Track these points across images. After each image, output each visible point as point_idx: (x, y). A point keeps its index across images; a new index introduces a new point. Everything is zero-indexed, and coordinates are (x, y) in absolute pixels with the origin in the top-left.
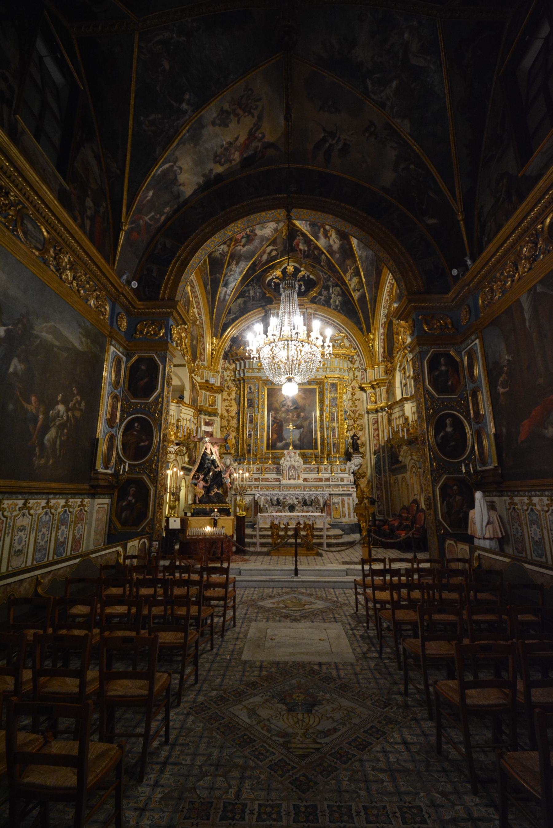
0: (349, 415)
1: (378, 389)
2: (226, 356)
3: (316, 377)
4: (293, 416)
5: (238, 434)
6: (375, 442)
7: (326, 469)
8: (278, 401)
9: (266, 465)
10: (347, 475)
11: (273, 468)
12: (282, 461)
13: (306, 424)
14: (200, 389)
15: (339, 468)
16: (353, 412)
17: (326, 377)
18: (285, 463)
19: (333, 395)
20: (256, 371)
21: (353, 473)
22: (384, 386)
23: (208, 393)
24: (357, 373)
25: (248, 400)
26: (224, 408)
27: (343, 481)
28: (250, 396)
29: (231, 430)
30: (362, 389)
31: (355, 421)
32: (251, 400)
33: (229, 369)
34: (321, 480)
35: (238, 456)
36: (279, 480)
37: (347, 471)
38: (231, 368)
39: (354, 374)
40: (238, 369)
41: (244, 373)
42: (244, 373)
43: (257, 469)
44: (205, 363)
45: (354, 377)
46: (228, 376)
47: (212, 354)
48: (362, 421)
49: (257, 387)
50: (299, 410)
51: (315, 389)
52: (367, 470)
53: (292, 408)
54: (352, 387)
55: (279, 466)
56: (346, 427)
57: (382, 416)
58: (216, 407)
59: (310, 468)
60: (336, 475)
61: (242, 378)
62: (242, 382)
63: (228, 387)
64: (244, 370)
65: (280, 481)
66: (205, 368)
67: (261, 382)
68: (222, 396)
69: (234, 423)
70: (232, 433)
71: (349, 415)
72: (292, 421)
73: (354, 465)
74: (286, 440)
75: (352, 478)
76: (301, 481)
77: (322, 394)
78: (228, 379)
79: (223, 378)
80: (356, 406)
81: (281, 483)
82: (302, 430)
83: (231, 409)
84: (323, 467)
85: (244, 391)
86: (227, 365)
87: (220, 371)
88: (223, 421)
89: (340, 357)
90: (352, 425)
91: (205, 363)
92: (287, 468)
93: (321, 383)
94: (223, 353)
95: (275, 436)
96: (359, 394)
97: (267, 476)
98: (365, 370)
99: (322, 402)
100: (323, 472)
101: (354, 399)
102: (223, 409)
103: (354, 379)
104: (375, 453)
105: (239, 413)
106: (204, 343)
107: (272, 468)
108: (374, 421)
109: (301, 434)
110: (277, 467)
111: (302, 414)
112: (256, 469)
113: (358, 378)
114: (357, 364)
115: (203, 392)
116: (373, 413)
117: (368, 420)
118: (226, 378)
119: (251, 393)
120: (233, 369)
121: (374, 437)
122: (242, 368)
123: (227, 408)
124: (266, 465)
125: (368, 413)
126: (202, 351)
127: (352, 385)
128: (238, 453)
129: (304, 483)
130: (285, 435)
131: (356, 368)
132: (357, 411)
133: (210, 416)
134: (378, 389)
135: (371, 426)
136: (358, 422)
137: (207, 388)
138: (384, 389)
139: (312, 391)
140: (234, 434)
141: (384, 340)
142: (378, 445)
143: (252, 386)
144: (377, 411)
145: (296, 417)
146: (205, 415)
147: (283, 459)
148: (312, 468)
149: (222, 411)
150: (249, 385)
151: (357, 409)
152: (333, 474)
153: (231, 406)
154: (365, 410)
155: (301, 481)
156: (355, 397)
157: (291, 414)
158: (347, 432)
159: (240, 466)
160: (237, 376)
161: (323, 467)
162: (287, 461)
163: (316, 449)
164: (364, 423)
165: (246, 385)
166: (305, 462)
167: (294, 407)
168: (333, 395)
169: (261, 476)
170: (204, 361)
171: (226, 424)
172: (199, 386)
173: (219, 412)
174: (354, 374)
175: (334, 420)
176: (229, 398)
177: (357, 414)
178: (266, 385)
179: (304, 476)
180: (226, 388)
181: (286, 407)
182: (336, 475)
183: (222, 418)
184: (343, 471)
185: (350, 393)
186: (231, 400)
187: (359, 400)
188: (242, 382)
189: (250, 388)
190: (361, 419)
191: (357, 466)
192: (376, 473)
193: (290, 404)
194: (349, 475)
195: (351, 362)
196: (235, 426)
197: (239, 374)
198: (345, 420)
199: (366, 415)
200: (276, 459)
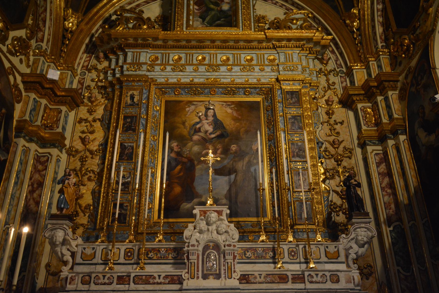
0: (326, 150)
1: (380, 98)
2: (92, 49)
3: (259, 80)
5: (100, 186)
6: (386, 198)
7: (293, 254)
8: (187, 124)
9: (149, 245)
10: (343, 267)
11: (167, 250)
12: (187, 233)
13: (241, 165)
14: (26, 90)
15: (322, 249)
16: (333, 144)
17: (278, 80)
18: (196, 235)
19: (293, 111)
20: (145, 67)
21: (355, 261)
22: (394, 89)
23: (44, 102)
24: (332, 79)
25: (125, 118)
26: (78, 134)
27: (338, 281)
28: (131, 111)
30: (347, 102)
31: (338, 162)
32: (132, 117)
33: (96, 69)
34: (283, 279)
35: (95, 229)
36: (179, 280)
37: (342, 258)
38: (100, 67)
39: (328, 80)
40: (113, 67)
41: (122, 72)
42: (122, 72)
43: (128, 254)
44: (44, 45)
45: (329, 85)
46: (93, 80)
47: (64, 37)
48: (353, 161)
49: (145, 96)
50: (226, 140)
51: (258, 103)
52: (374, 260)
53: (213, 136)
54: (327, 101)
55: (179, 245)
56: (323, 171)
57: (397, 148)
58: (60, 130)
59: (255, 250)
60: (320, 267)
61: (118, 79)
62: (117, 87)
63: (89, 98)
64: (122, 67)
65: (181, 283)
66: (43, 54)
67: (153, 88)
68: (76, 114)
69: (94, 164)
70: (89, 183)
71: (326, 150)
73: (356, 243)
74: (201, 197)
75: (356, 274)
76: (234, 283)
77: (271, 110)
78: (93, 85)
79: (82, 84)
80: (338, 133)
81: (185, 286)
82: (233, 176)
83: (91, 137)
84: (286, 248)
85: (120, 103)
86: (94, 61)
87: (79, 72)
88: (72, 159)
89: (302, 47)
90: (333, 169)
91: (44, 45)
92: (201, 248)
93: (269, 92)
94: (87, 41)
95: (178, 189)
96: (340, 112)
97: (150, 269)
98: (350, 73)
99: (272, 124)
100: (286, 259)
102: (76, 137)
103: (329, 88)
104: (389, 222)
105: (104, 145)
106: (46, 10)
107: (163, 251)
108: (377, 158)
109: (232, 185)
110: (175, 250)
111: (234, 147)
112: (126, 254)
114: (331, 65)
115: (33, 96)
116: (375, 144)
117: (365, 160)
118: (88, 82)
119: (133, 105)
120: (104, 69)
121: (383, 189)
122: (120, 63)
123: (83, 136)
124: (149, 245)
125: (363, 146)
126: (41, 23)
127: (326, 98)
128: (95, 223)
129: (241, 286)
131: (331, 71)
133: (43, 146)
134: (380, 98)
135: (373, 167)
136: (344, 163)
137: (41, 90)
138: (393, 95)
139: (254, 106)
140: (92, 185)
141: (384, 10)
142: (393, 206)
143: (135, 93)
144: (382, 139)
146: (30, 141)
147: (191, 226)
148: (260, 251)
149: (72, 140)
150: (131, 92)
152: (312, 265)
153: (92, 132)
154: (356, 142)
155: (234, 283)
156: (334, 117)
158: (324, 181)
159: (87, 245)
160: (110, 78)
161: (284, 247)
162: (201, 232)
163: (264, 215)
164: (357, 164)
165: (124, 91)
166: (242, 239)
167: (218, 133)
168: (293, 111)
169: (134, 271)
170: (42, 41)
171: (78, 165)
172: (23, 82)
173: (67, 142)
174: (328, 80)
178: (164, 93)
179: (240, 269)
180: (85, 101)
181: (202, 134)
182: (320, 267)
183: (71, 152)
184: (333, 257)
185: (324, 111)
187: (342, 123)
188: (117, 87)
189: (132, 97)
190: (350, 158)
191: (362, 246)
192: (398, 265)
193: (210, 129)
194: (348, 266)
195: (321, 61)
196: (96, 169)
197: (114, 74)
198: (320, 158)
199: (359, 151)
200: (175, 234)
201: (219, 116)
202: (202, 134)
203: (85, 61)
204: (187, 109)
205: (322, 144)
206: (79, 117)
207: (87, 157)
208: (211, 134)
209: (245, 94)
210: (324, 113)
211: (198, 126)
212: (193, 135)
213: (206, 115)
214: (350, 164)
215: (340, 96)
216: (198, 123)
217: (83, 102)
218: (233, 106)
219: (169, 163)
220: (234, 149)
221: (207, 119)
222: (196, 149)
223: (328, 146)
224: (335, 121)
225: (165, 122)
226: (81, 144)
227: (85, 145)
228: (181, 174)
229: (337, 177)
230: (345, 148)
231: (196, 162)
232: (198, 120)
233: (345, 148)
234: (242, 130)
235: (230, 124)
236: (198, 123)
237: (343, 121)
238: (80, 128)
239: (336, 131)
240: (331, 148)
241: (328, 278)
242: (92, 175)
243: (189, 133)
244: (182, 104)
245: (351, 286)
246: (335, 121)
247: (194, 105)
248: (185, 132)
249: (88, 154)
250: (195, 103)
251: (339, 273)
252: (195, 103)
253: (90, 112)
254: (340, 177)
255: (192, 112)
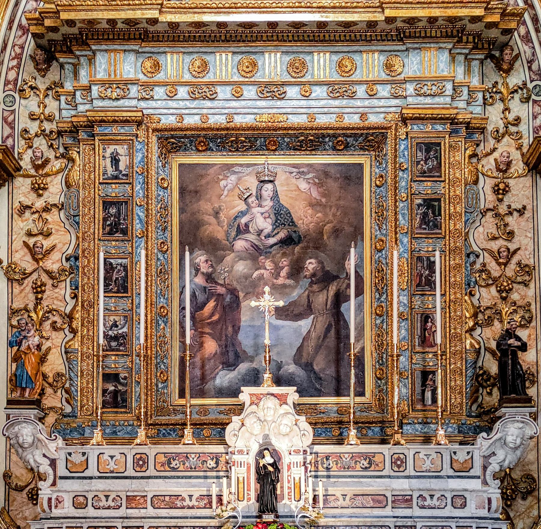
4: (277, 270)
8: (222, 215)
26: (19, 239)
29: (47, 325)
31: (504, 293)
39: (507, 109)
46: (32, 117)
50: (297, 249)
51: (361, 166)
53: (272, 241)
70: (54, 334)
71: (484, 269)
72: (275, 288)
88: (17, 289)
101: (503, 209)
113: (523, 128)
118: (23, 122)
123: (31, 241)
130: (245, 340)
132: (512, 254)
136: (515, 296)
145: (290, 276)
151: (512, 247)
157: (269, 265)
167: (282, 235)
175: (431, 284)
176: (39, 204)
177: (511, 270)
181: (251, 237)
186: (46, 209)
187: (521, 212)
190: (526, 284)
193: (267, 226)
201: (284, 201)
202: (251, 237)
203: (9, 69)
204: (223, 183)
205: (478, 256)
206: (16, 205)
207: (43, 284)
208: (268, 236)
209: (334, 148)
210: (488, 190)
211: (244, 220)
212: (234, 239)
213: (259, 197)
214: (523, 297)
215: (525, 150)
216: (243, 214)
217: (18, 169)
218: (310, 176)
219: (193, 295)
220: (311, 267)
221: (260, 206)
222: (241, 267)
223: (488, 259)
224: (509, 207)
225: (182, 210)
226: (29, 258)
227: (37, 261)
228: (215, 318)
229: (496, 323)
230: (519, 264)
231: (241, 295)
232: (242, 207)
233: (519, 264)
234: (328, 227)
235: (305, 218)
236: (243, 214)
237: (524, 208)
238: (22, 225)
239: (508, 229)
240: (494, 263)
241: (449, 500)
242: (57, 318)
243: (227, 234)
244: (212, 171)
245: (484, 513)
246: (509, 207)
247: (235, 173)
248: (220, 234)
249: (45, 278)
250: (236, 169)
251: (466, 495)
252: (236, 169)
253: (38, 189)
254: (501, 322)
255: (232, 190)
